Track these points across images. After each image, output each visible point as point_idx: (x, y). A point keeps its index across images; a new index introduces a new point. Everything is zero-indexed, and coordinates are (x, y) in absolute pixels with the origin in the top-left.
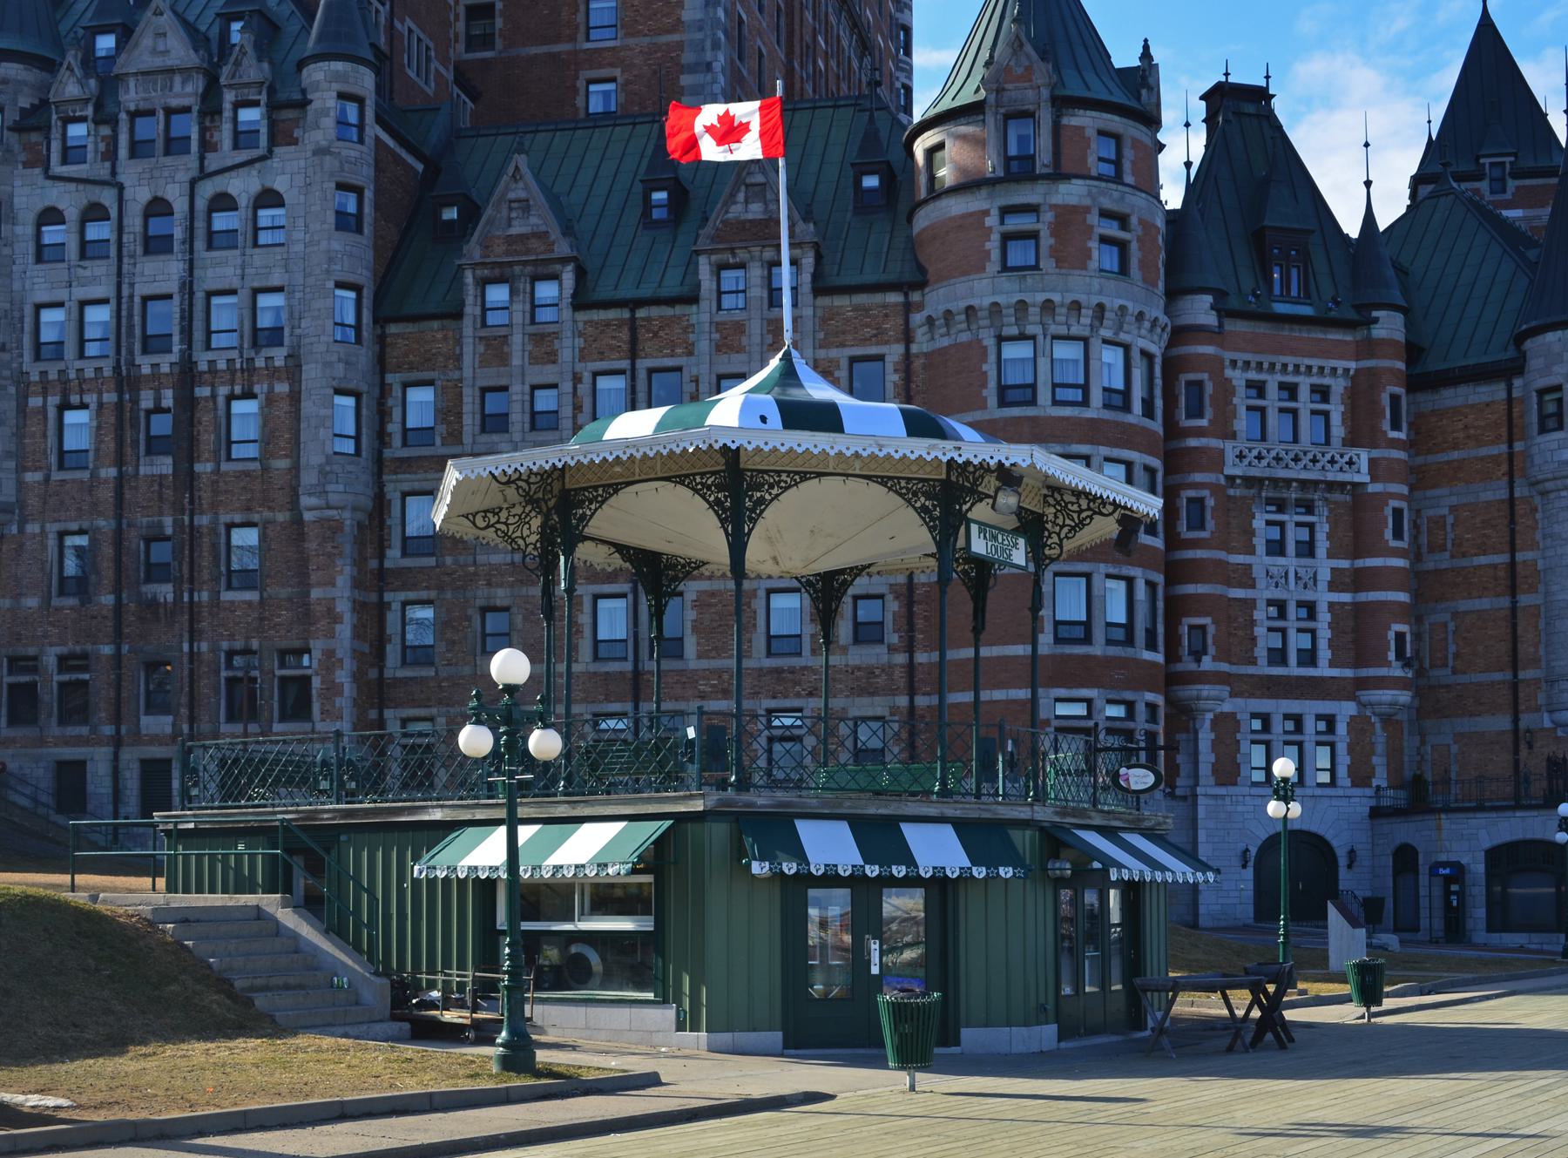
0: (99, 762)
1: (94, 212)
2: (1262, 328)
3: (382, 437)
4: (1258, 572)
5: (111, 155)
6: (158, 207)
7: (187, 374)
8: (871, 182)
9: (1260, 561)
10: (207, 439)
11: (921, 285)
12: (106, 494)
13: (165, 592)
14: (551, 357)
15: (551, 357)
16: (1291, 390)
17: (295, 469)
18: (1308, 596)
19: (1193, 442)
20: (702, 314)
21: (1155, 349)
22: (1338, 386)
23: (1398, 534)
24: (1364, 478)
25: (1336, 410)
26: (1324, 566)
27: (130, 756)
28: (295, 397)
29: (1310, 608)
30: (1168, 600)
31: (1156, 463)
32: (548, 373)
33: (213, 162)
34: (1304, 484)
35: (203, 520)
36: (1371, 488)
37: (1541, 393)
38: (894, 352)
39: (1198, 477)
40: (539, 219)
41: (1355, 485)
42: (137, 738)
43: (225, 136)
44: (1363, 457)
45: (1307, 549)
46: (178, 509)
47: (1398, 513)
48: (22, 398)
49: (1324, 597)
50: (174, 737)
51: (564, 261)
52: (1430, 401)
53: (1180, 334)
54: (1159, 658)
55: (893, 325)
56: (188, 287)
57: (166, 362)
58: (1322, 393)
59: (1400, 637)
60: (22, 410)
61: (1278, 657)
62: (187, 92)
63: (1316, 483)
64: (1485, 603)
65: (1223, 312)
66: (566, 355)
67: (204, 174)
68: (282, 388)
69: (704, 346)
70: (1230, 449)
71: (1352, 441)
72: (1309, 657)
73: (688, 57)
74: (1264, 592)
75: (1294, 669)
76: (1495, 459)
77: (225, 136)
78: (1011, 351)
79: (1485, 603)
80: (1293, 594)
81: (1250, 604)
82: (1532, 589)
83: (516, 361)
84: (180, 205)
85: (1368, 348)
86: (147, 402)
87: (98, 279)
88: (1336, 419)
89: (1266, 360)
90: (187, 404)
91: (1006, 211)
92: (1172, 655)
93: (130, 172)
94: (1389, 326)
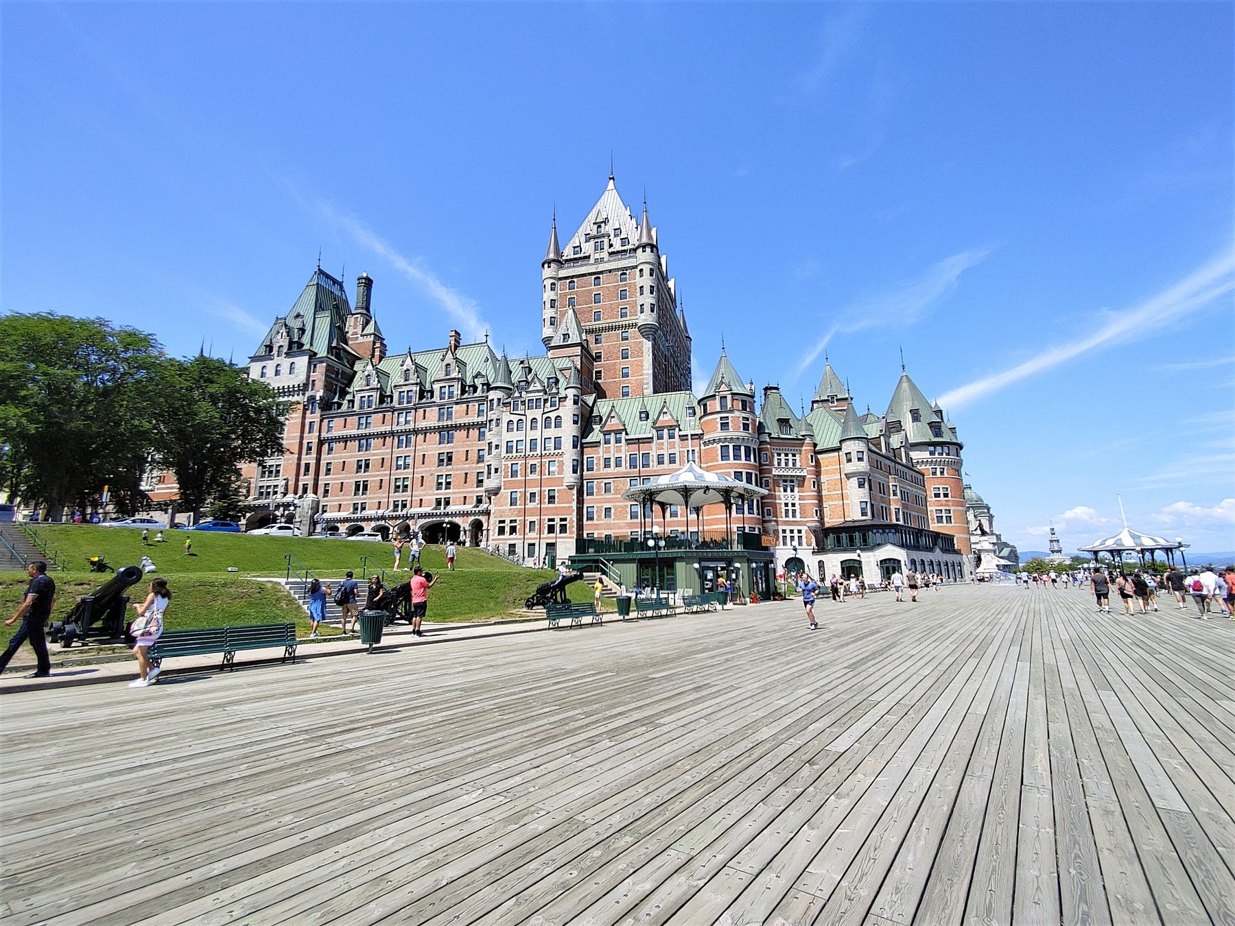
2: (780, 441)
3: (582, 470)
4: (782, 497)
18: (793, 502)
19: (765, 467)
21: (756, 447)
23: (814, 487)
24: (805, 474)
27: (527, 542)
29: (793, 505)
30: (762, 503)
31: (758, 473)
34: (791, 476)
36: (808, 476)
37: (846, 454)
39: (767, 475)
41: (804, 477)
43: (548, 404)
45: (792, 491)
47: (814, 482)
49: (797, 502)
51: (623, 430)
52: (819, 456)
53: (761, 443)
54: (761, 517)
59: (816, 511)
61: (787, 516)
63: (794, 476)
64: (836, 503)
65: (771, 438)
66: (623, 451)
69: (654, 448)
72: (794, 516)
73: (645, 381)
75: (791, 519)
76: (836, 469)
77: (548, 404)
79: (836, 503)
80: (790, 501)
81: (781, 504)
82: (847, 499)
83: (612, 452)
88: (798, 461)
89: (781, 448)
91: (721, 418)
92: (763, 516)
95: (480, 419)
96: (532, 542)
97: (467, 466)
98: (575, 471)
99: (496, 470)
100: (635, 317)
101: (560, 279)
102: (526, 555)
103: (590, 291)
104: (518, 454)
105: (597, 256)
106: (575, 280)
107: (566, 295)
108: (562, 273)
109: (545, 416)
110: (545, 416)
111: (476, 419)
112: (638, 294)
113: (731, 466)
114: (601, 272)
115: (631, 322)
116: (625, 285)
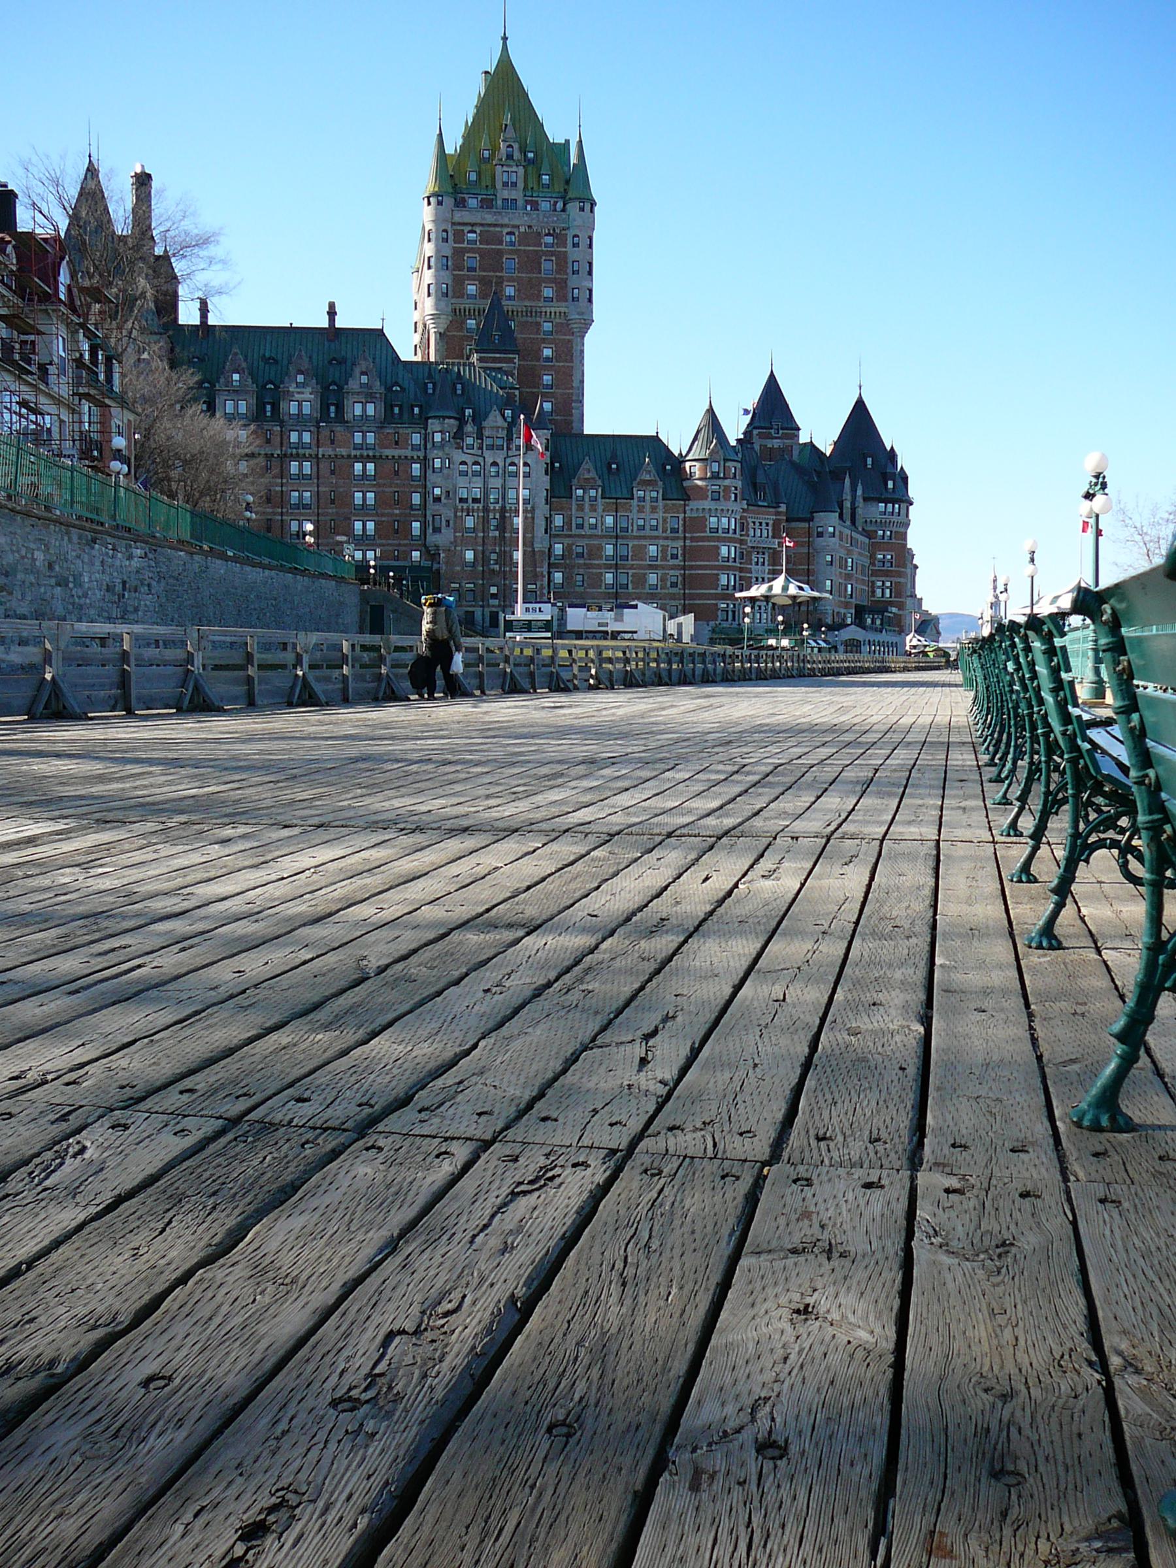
0: (478, 612)
1: (476, 463)
5: (481, 448)
6: (495, 464)
7: (503, 510)
8: (668, 467)
9: (753, 567)
10: (508, 527)
11: (689, 500)
12: (480, 541)
13: (497, 567)
14: (595, 511)
15: (595, 511)
16: (761, 524)
17: (533, 537)
20: (635, 502)
22: (771, 522)
25: (770, 528)
26: (767, 568)
28: (533, 518)
32: (595, 514)
33: (510, 453)
35: (507, 549)
38: (681, 516)
40: (593, 474)
42: (488, 606)
44: (777, 541)
45: (763, 564)
46: (500, 545)
48: (456, 513)
50: (499, 606)
55: (681, 509)
56: (504, 487)
57: (498, 507)
58: (767, 524)
60: (456, 516)
62: (503, 434)
67: (508, 456)
68: (529, 515)
69: (635, 511)
70: (749, 539)
71: (773, 537)
74: (754, 575)
78: (712, 519)
84: (501, 464)
85: (778, 513)
86: (491, 516)
87: (478, 482)
90: (503, 517)
93: (487, 454)
94: (783, 508)
95: (415, 454)
96: (494, 609)
97: (397, 512)
98: (546, 532)
99: (448, 521)
100: (564, 304)
101: (453, 224)
102: (487, 624)
103: (500, 253)
104: (476, 506)
105: (506, 194)
106: (478, 230)
107: (462, 251)
108: (458, 217)
109: (509, 461)
110: (509, 461)
111: (408, 453)
112: (570, 271)
113: (719, 539)
114: (518, 227)
115: (558, 310)
116: (552, 253)
